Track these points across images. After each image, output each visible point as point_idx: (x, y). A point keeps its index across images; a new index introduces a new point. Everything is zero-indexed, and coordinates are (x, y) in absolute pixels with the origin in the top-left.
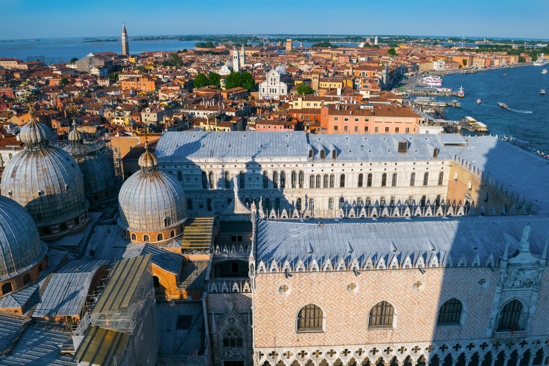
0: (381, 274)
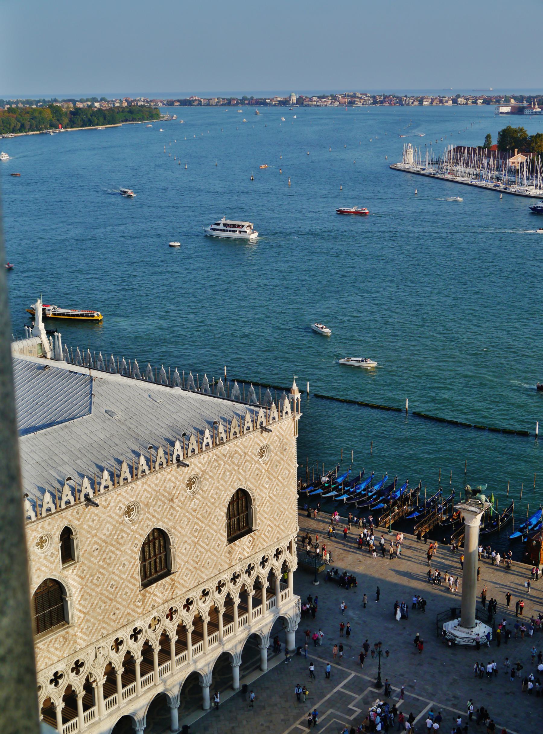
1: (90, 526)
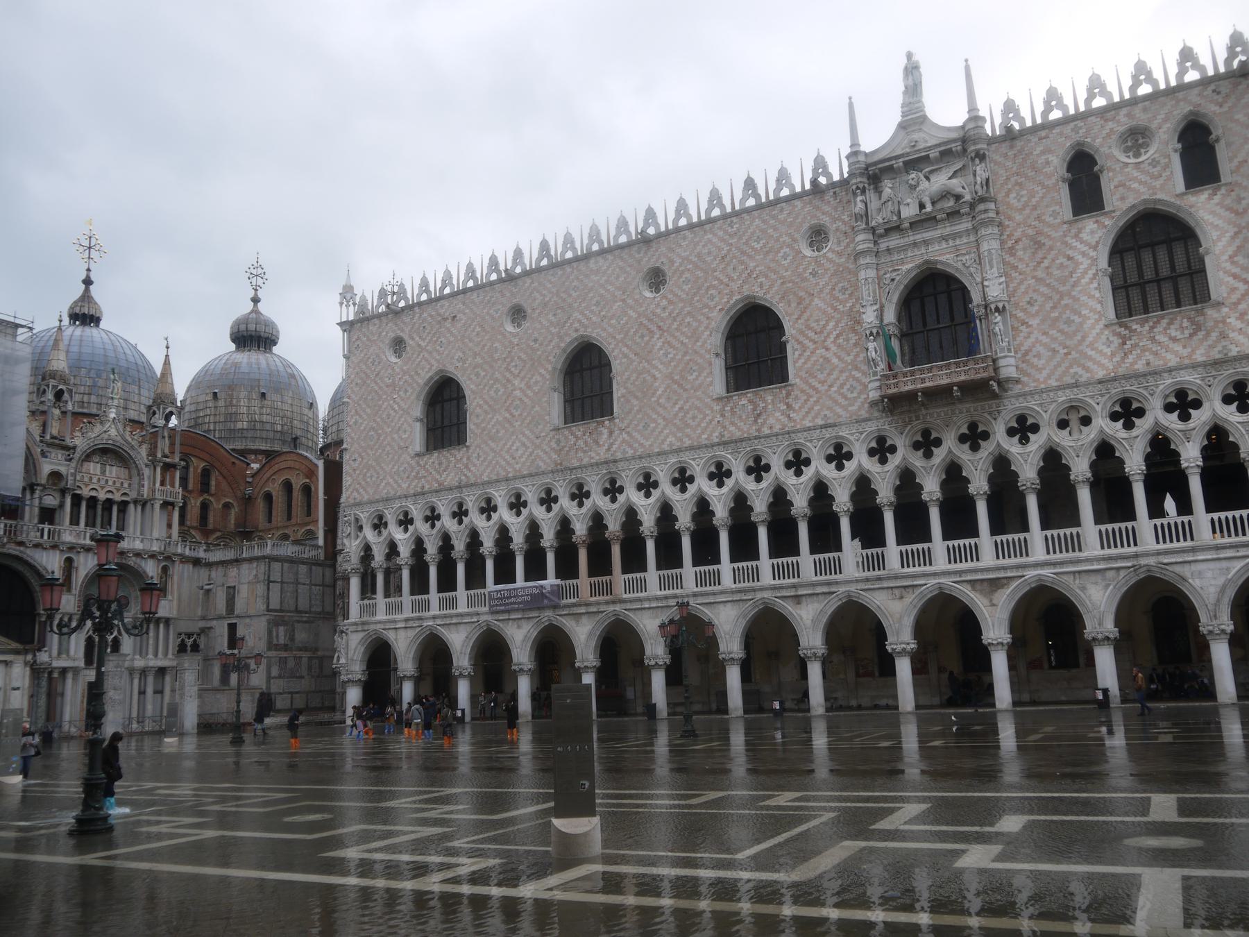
0: (569, 270)
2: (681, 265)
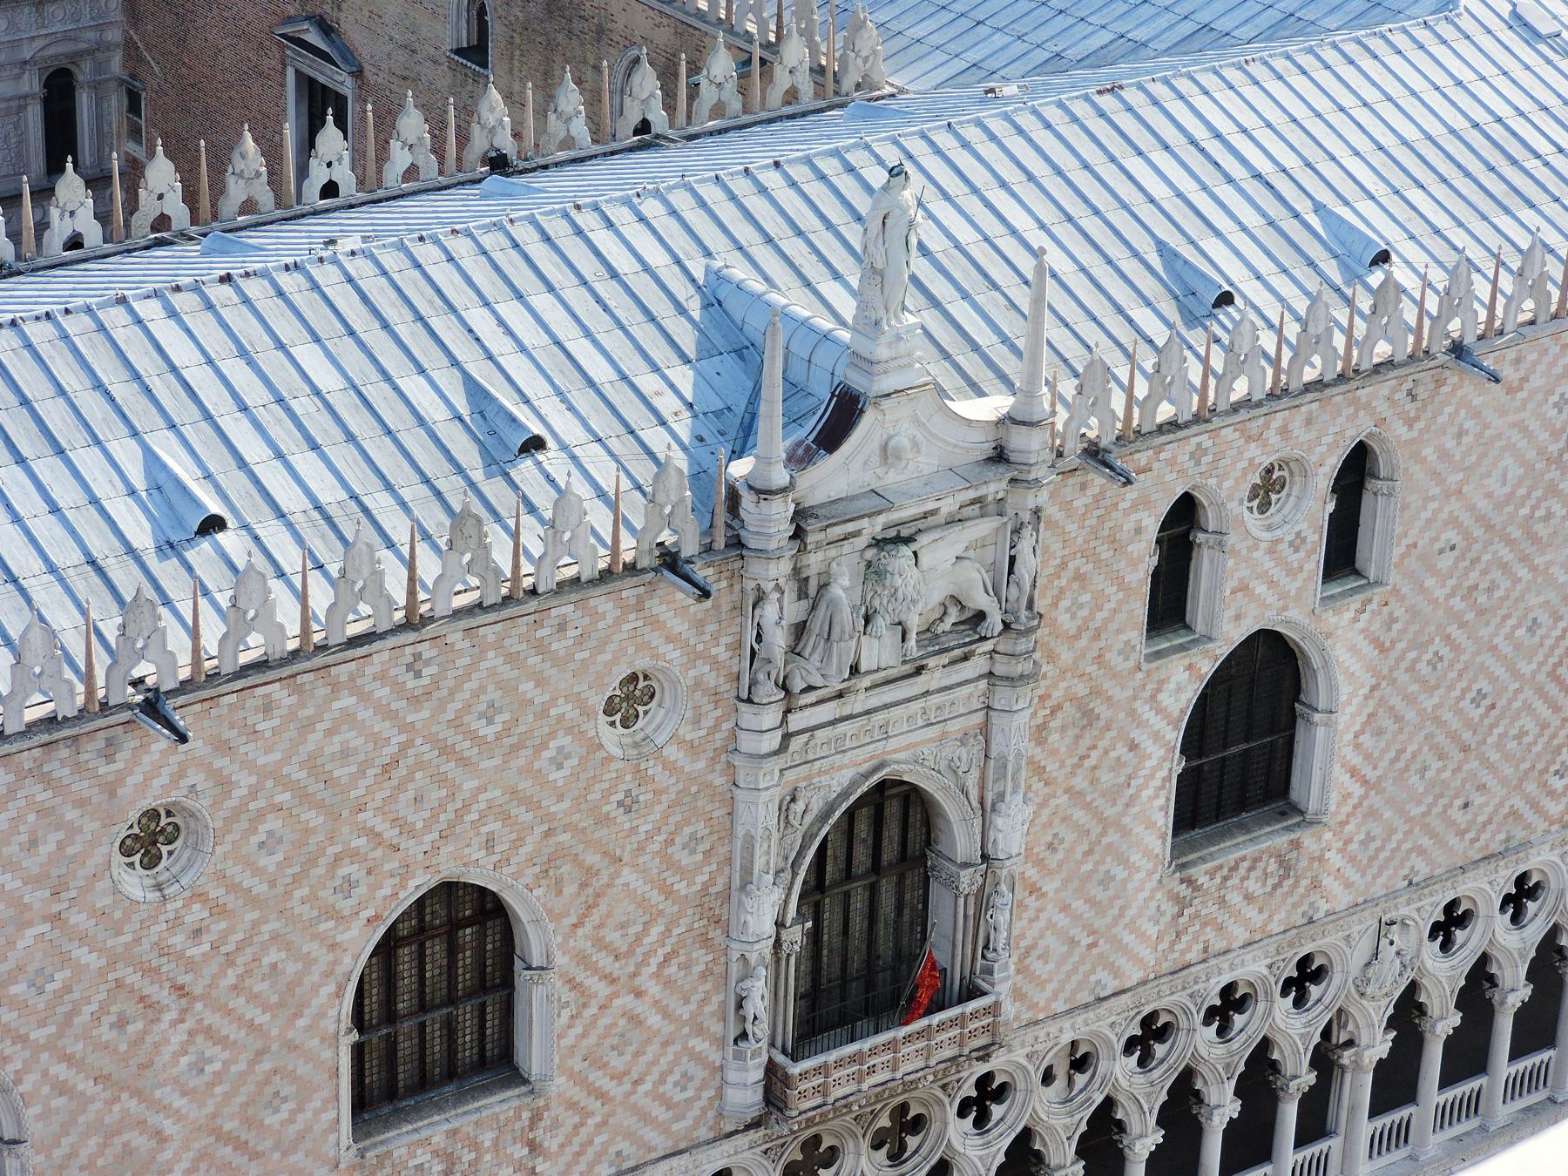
1: (1444, 455)
2: (253, 794)
